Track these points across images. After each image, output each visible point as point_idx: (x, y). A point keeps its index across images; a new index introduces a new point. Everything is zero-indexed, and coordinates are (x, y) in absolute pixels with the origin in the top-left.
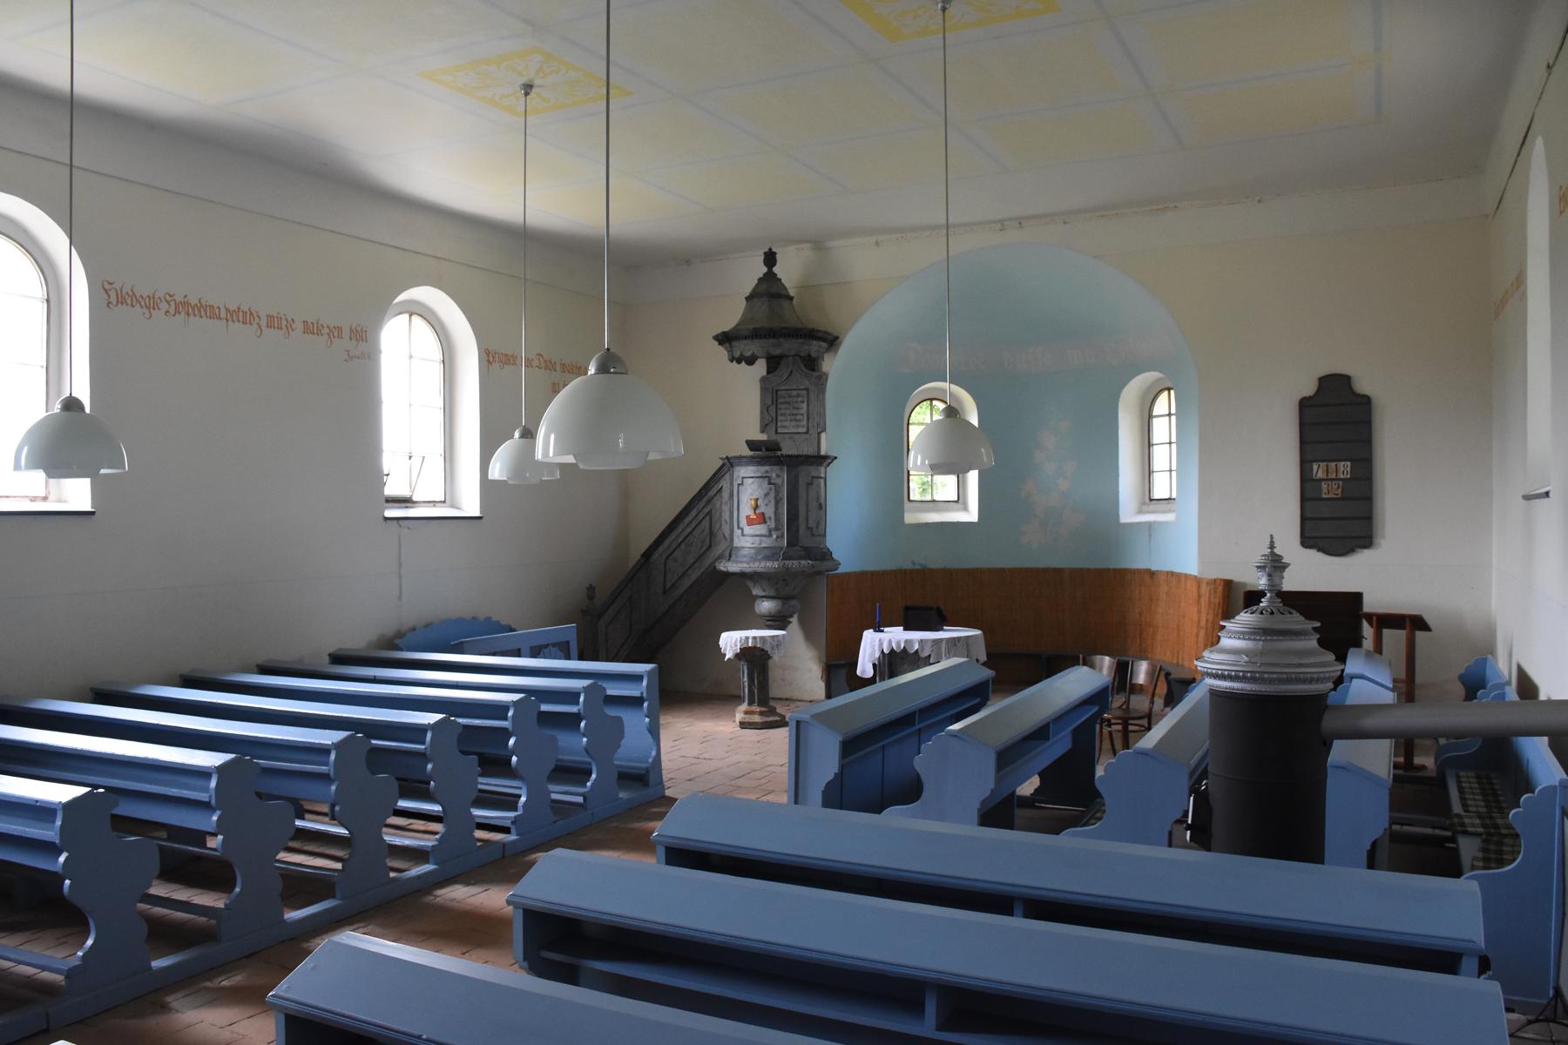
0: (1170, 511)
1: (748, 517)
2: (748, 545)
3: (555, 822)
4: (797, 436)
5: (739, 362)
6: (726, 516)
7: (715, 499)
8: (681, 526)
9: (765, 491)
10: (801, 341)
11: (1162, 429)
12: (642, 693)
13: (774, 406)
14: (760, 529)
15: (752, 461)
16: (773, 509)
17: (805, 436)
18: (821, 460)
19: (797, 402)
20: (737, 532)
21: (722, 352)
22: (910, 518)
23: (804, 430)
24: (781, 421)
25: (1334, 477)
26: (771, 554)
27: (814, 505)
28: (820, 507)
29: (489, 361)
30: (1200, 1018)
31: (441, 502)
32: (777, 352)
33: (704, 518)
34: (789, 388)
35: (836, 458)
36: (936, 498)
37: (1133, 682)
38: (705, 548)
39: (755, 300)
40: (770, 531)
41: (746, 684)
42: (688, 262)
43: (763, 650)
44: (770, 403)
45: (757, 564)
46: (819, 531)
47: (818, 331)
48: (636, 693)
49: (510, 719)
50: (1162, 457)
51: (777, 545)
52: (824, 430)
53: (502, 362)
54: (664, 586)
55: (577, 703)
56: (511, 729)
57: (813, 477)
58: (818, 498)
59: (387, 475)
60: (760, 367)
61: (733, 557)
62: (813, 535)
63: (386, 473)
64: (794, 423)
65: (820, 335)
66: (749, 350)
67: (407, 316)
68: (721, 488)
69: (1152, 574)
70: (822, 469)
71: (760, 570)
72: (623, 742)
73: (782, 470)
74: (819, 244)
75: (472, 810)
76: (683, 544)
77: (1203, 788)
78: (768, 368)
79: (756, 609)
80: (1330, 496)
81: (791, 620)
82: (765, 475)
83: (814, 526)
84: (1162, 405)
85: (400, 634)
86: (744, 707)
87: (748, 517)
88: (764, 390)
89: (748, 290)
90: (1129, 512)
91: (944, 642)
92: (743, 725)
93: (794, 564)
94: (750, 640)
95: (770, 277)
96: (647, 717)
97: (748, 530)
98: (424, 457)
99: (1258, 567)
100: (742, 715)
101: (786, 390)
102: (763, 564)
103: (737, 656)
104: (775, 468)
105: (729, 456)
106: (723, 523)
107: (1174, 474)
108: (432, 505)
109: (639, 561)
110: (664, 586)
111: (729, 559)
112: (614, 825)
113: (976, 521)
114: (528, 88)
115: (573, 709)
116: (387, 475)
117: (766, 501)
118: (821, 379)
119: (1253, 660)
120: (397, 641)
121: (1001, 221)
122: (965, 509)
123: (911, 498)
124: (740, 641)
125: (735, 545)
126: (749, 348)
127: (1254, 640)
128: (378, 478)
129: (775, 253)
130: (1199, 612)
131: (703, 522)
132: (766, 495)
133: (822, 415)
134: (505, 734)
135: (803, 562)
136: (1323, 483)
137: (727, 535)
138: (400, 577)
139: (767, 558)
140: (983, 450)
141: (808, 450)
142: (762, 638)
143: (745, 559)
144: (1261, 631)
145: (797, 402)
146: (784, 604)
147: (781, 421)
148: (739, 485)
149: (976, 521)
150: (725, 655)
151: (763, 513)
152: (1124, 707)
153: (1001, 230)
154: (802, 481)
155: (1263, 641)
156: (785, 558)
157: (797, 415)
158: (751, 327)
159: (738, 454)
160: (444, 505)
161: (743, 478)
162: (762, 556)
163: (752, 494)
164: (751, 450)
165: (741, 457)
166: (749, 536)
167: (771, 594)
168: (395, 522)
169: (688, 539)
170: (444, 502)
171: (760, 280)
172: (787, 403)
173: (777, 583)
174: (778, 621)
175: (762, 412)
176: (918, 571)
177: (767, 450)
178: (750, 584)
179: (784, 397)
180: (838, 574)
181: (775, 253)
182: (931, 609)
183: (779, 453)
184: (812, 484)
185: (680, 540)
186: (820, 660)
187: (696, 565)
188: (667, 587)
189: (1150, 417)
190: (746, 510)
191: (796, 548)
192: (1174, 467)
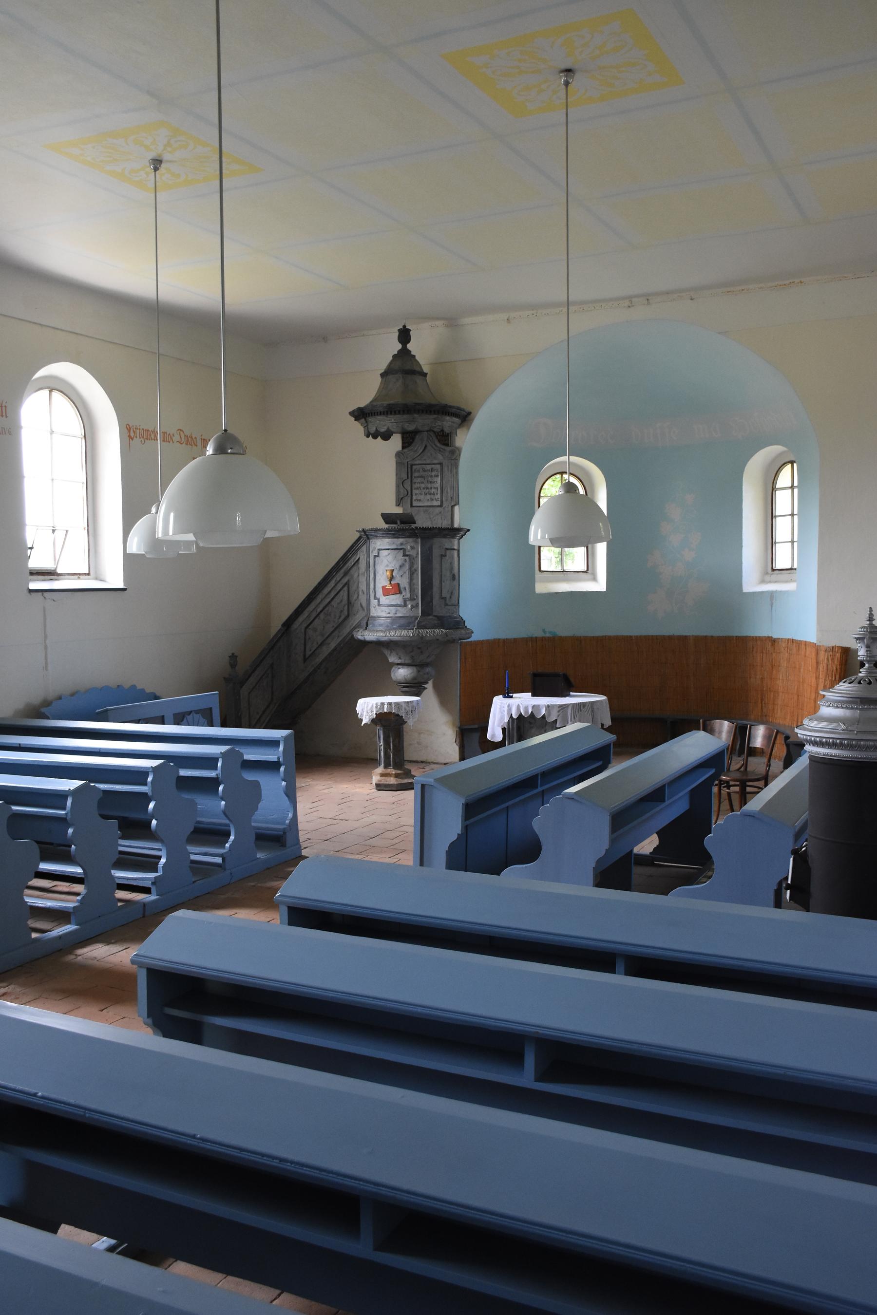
0: (791, 581)
1: (384, 588)
2: (384, 614)
3: (194, 882)
4: (431, 509)
5: (375, 437)
6: (363, 587)
7: (352, 571)
8: (320, 597)
9: (400, 563)
10: (435, 416)
11: (784, 502)
12: (279, 758)
13: (409, 479)
14: (396, 599)
15: (388, 533)
16: (408, 580)
17: (439, 509)
18: (455, 532)
19: (431, 476)
20: (374, 602)
21: (358, 428)
22: (541, 588)
23: (439, 503)
24: (416, 494)
26: (406, 623)
27: (447, 574)
28: (453, 577)
29: (130, 436)
30: (782, 1072)
31: (85, 574)
32: (411, 428)
33: (344, 586)
34: (424, 462)
35: (468, 530)
36: (566, 568)
37: (751, 746)
38: (343, 617)
39: (390, 377)
40: (405, 601)
41: (382, 748)
42: (325, 339)
43: (398, 715)
44: (404, 476)
45: (392, 633)
46: (452, 600)
47: (451, 407)
48: (273, 758)
49: (149, 784)
50: (784, 529)
51: (412, 615)
52: (457, 503)
53: (143, 437)
54: (305, 655)
55: (216, 768)
56: (150, 794)
57: (447, 549)
58: (452, 569)
59: (31, 548)
60: (396, 442)
61: (370, 626)
62: (446, 605)
63: (29, 545)
64: (428, 497)
65: (453, 410)
66: (384, 425)
67: (46, 392)
68: (359, 558)
69: (773, 641)
70: (456, 541)
71: (396, 638)
72: (260, 805)
73: (416, 542)
74: (452, 322)
75: (113, 872)
76: (322, 613)
77: (803, 849)
78: (403, 443)
79: (392, 675)
81: (426, 686)
82: (399, 547)
83: (448, 596)
84: (785, 478)
85: (47, 703)
86: (380, 769)
87: (384, 588)
88: (399, 464)
89: (383, 366)
90: (751, 583)
91: (570, 708)
92: (380, 787)
93: (428, 633)
94: (386, 707)
95: (404, 354)
96: (283, 780)
97: (384, 600)
98: (67, 531)
99: (857, 639)
100: (378, 778)
101: (421, 464)
102: (398, 633)
103: (373, 721)
104: (410, 540)
105: (366, 528)
106: (360, 593)
107: (795, 544)
108: (76, 577)
109: (280, 630)
110: (305, 655)
111: (366, 629)
112: (252, 884)
113: (605, 590)
114: (157, 163)
115: (211, 774)
116: (31, 548)
117: (401, 573)
118: (454, 455)
119: (849, 728)
120: (43, 710)
121: (630, 298)
122: (594, 579)
123: (543, 568)
124: (376, 707)
125: (371, 615)
126: (383, 423)
127: (852, 708)
128: (22, 550)
129: (409, 331)
130: (817, 678)
131: (342, 591)
132: (401, 566)
133: (455, 488)
134: (145, 798)
135: (437, 631)
137: (364, 605)
138: (46, 648)
139: (401, 627)
140: (601, 524)
141: (441, 522)
142: (397, 704)
143: (381, 628)
144: (859, 700)
145: (431, 476)
146: (419, 671)
147: (416, 494)
148: (375, 557)
149: (605, 590)
150: (362, 720)
151: (398, 584)
152: (742, 769)
153: (629, 307)
154: (436, 552)
155: (860, 709)
156: (419, 627)
157: (431, 488)
158: (386, 403)
159: (374, 527)
160: (87, 577)
161: (379, 550)
162: (398, 625)
163: (387, 566)
164: (387, 523)
165: (376, 530)
166: (384, 606)
167: (407, 662)
168: (40, 593)
169: (327, 608)
170: (89, 574)
171: (394, 356)
172: (421, 477)
173: (412, 652)
174: (414, 687)
175: (397, 486)
176: (549, 639)
177: (402, 522)
178: (386, 652)
179: (419, 471)
180: (471, 641)
181: (409, 331)
182: (556, 675)
183: (414, 526)
185: (319, 610)
186: (454, 725)
187: (334, 634)
188: (307, 656)
189: (774, 489)
190: (382, 581)
191: (431, 617)
192: (796, 539)
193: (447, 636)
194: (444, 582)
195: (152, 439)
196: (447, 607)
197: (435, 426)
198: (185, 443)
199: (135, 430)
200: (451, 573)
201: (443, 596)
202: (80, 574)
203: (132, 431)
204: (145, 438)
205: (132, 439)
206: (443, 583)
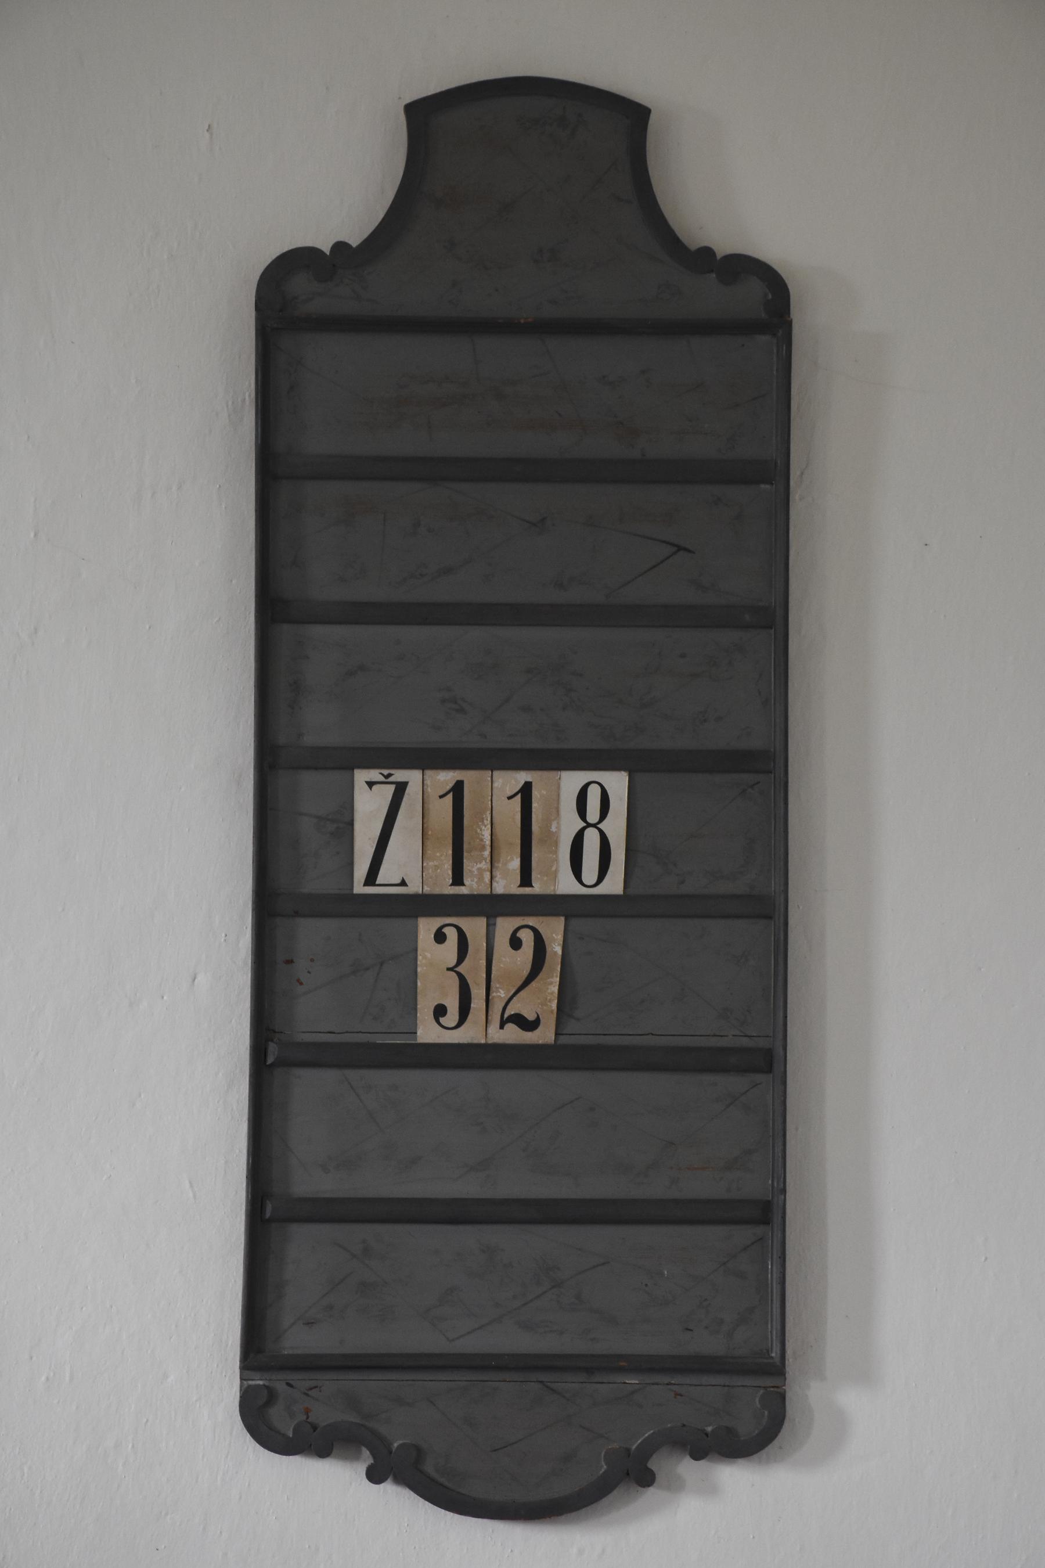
25: (507, 883)
80: (469, 1034)
136: (426, 927)
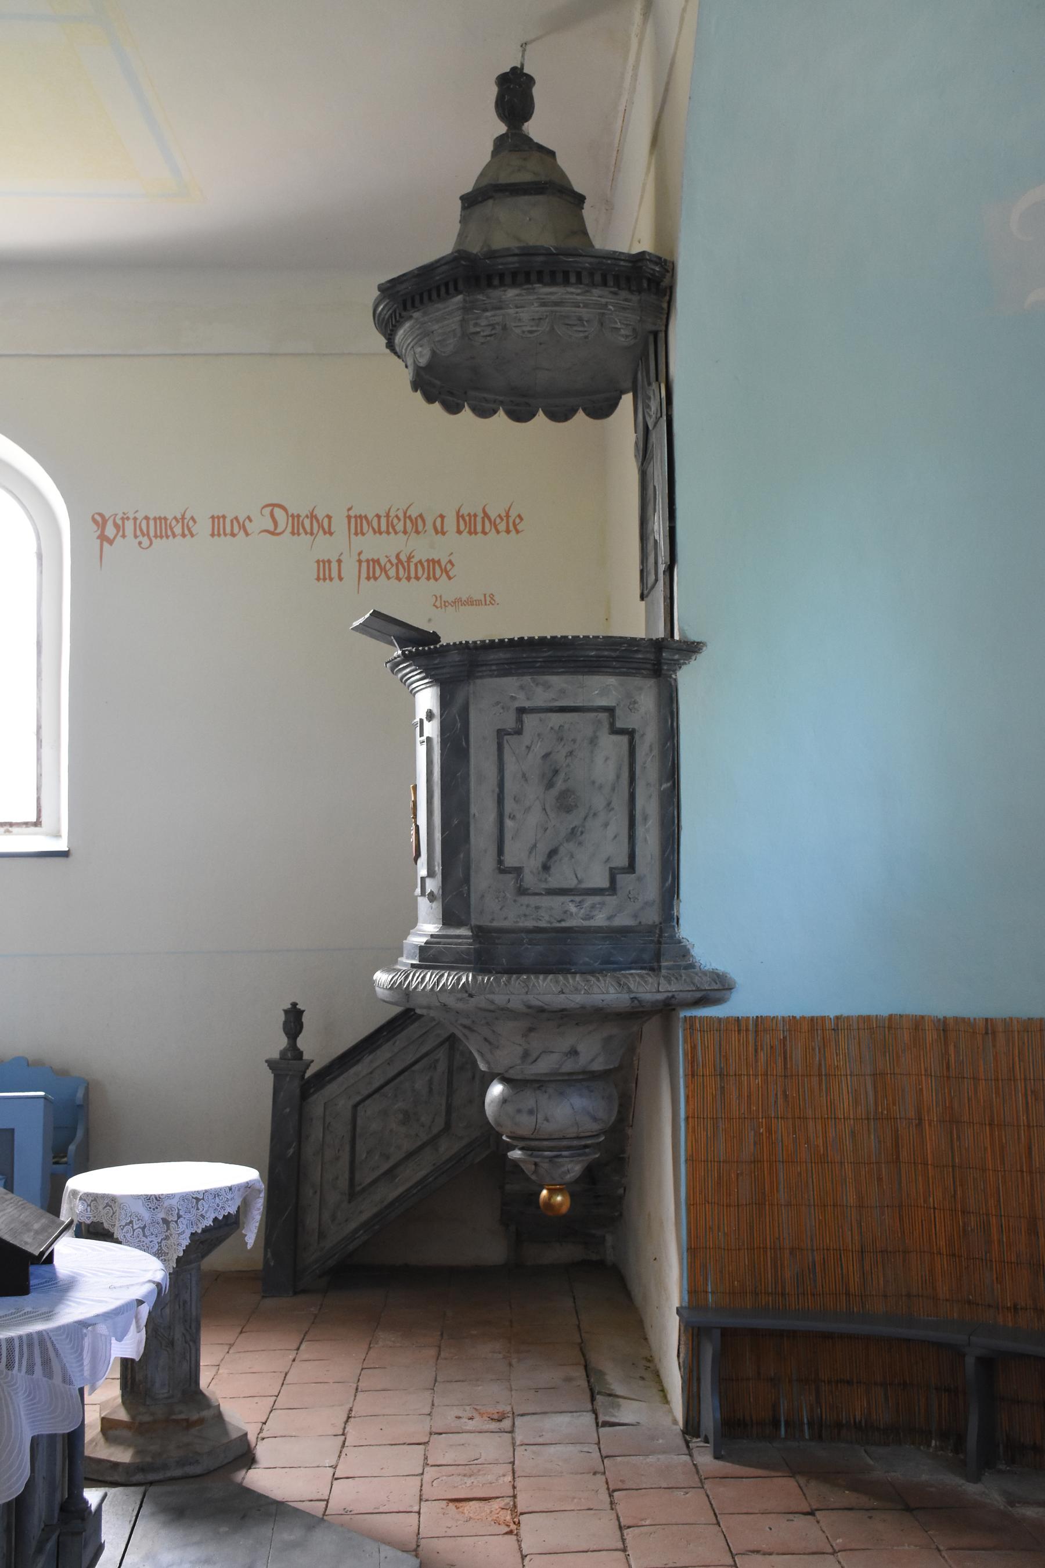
29: (103, 538)
31: (26, 824)
57: (521, 711)
62: (522, 891)
83: (532, 865)
160: (32, 829)
184: (519, 732)
193: (471, 996)
194: (512, 817)
195: (174, 536)
196: (525, 900)
197: (478, 329)
198: (289, 529)
199: (120, 522)
200: (550, 785)
201: (509, 861)
202: (11, 824)
203: (110, 524)
204: (152, 533)
205: (111, 542)
206: (509, 823)
